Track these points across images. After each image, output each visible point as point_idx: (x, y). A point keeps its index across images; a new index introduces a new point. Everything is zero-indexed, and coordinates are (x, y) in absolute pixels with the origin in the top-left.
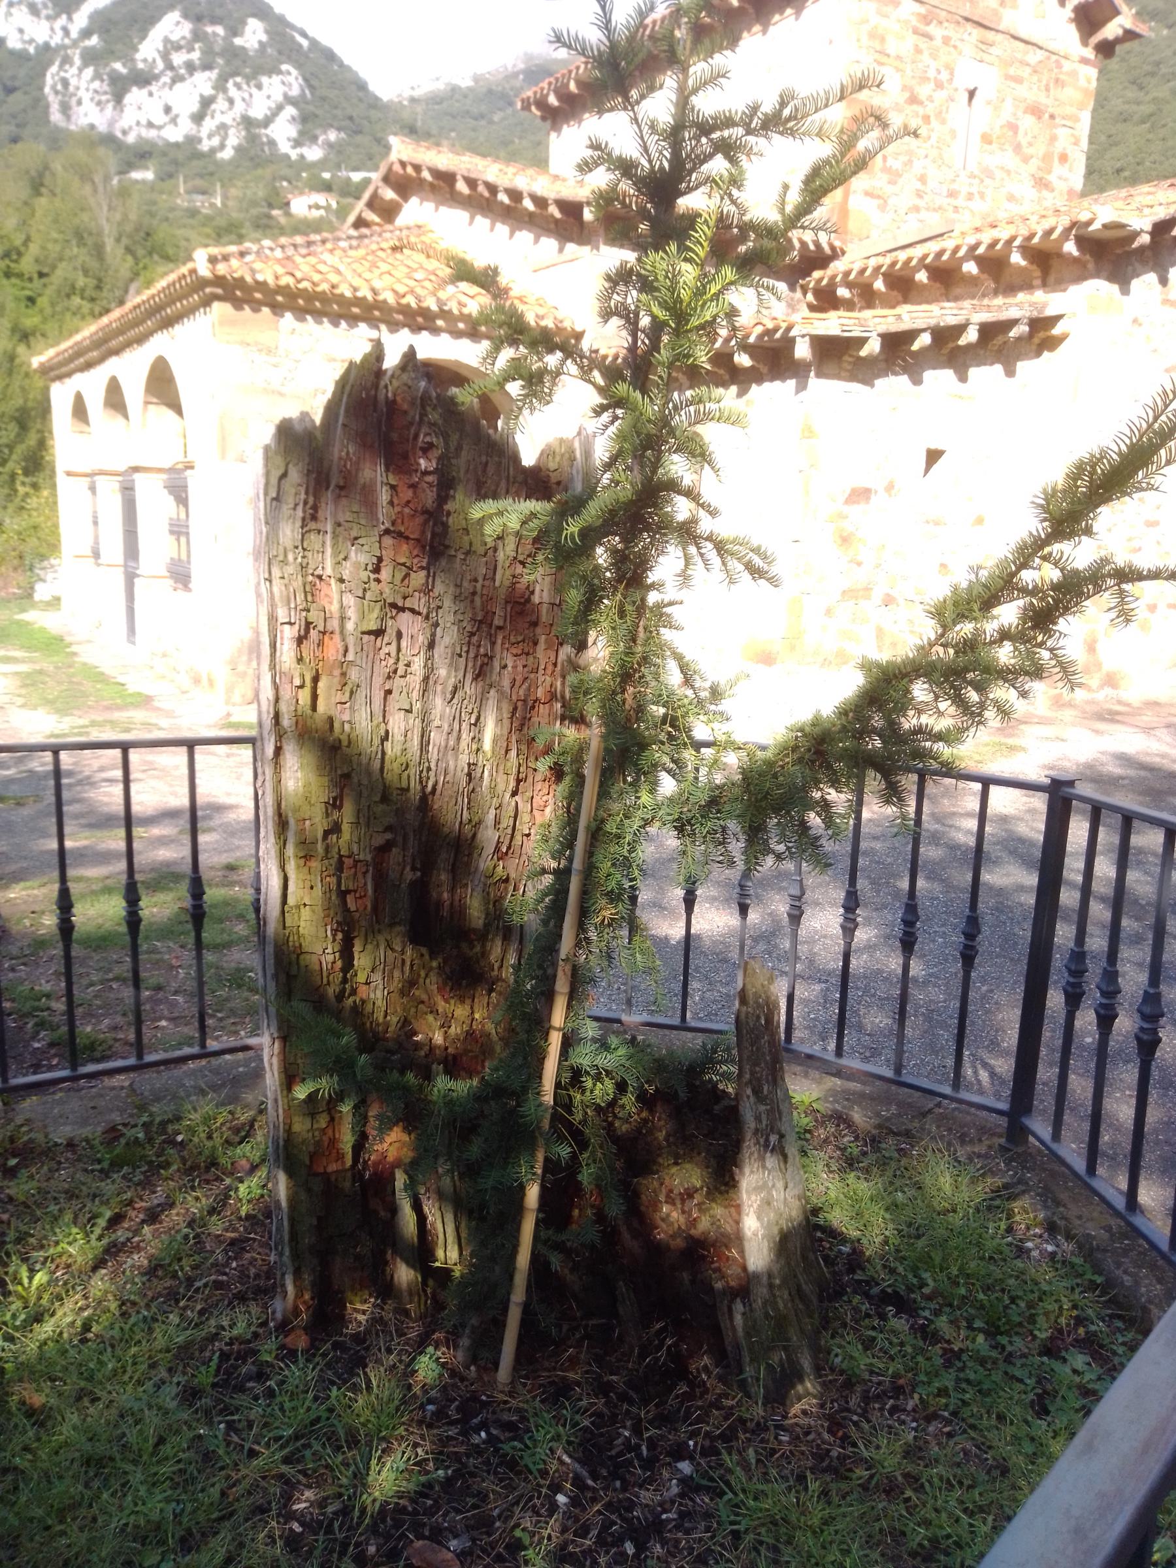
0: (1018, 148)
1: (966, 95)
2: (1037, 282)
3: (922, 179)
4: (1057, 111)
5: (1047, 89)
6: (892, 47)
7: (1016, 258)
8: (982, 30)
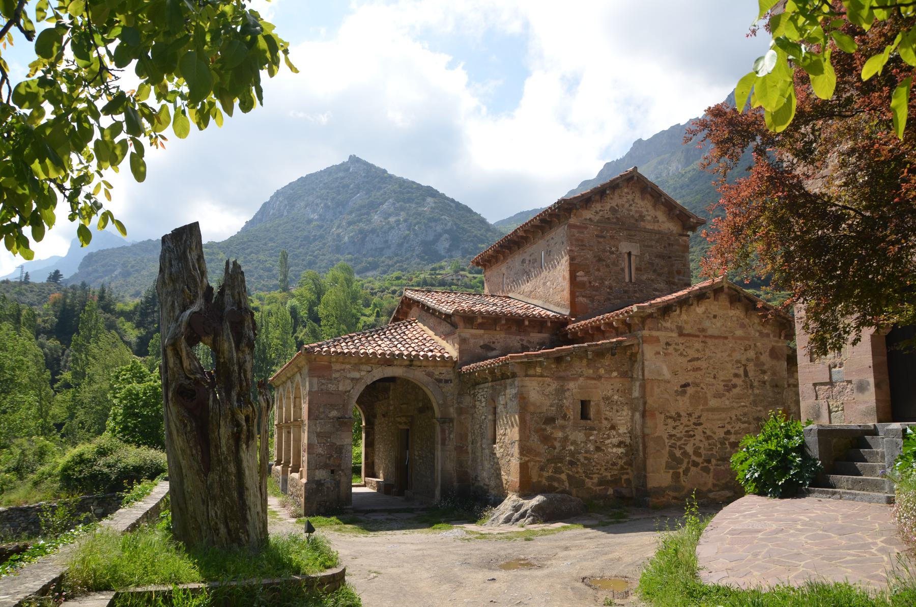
0: (655, 271)
1: (626, 256)
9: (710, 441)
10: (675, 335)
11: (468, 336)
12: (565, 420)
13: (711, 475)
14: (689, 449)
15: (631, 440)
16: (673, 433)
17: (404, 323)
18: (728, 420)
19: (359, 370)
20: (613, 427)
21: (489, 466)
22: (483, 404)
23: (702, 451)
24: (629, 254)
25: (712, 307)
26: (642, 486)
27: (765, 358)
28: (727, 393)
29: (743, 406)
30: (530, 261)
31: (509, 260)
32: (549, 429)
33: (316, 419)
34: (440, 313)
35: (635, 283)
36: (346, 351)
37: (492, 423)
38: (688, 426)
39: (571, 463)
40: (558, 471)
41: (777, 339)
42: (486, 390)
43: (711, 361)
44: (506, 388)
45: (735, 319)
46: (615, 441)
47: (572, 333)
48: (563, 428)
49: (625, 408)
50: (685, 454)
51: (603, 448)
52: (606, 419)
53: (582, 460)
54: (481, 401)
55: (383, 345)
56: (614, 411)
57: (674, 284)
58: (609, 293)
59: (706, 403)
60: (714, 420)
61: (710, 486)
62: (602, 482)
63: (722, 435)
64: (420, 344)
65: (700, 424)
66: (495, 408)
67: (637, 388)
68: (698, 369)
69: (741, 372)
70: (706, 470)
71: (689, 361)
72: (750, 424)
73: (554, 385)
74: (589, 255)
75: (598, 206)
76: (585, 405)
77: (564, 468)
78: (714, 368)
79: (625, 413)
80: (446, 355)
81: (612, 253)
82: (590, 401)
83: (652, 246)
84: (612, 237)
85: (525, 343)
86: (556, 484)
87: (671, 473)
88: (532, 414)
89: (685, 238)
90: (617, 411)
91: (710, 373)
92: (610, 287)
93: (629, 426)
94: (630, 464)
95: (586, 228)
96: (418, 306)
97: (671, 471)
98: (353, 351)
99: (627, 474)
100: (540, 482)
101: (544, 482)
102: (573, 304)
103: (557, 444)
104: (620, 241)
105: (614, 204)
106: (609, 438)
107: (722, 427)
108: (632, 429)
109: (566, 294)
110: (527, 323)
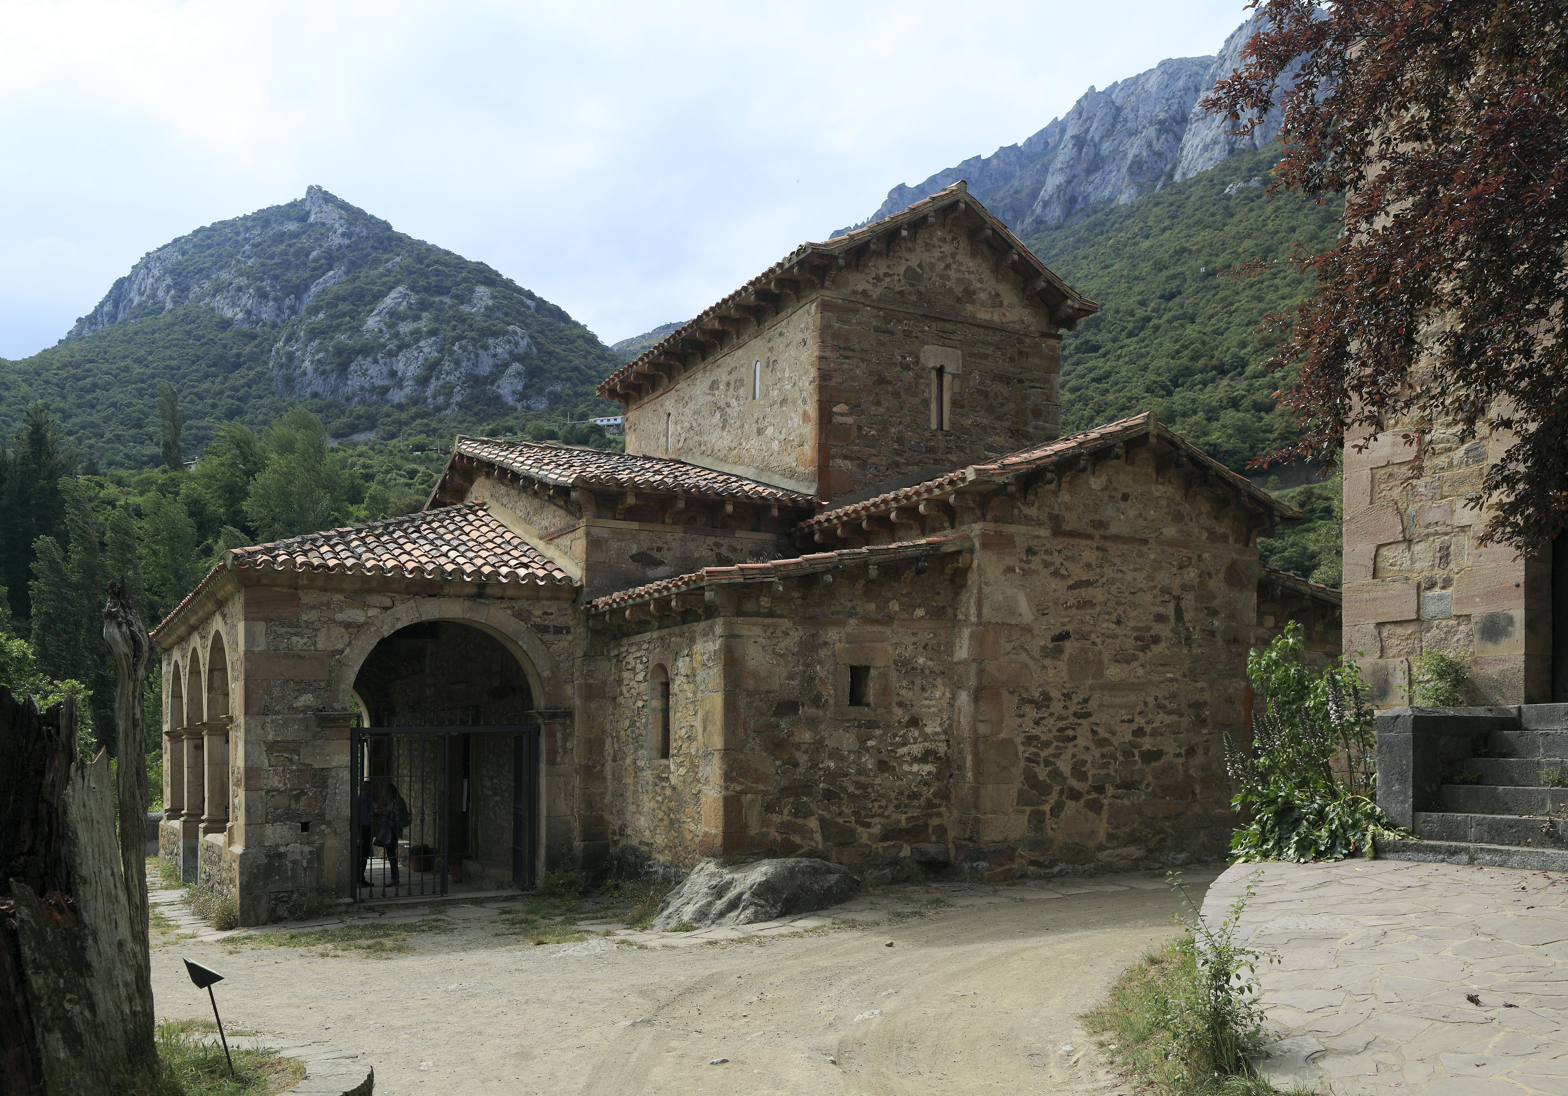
0: (990, 409)
1: (933, 375)
2: (947, 525)
3: (900, 441)
11: (604, 533)
12: (818, 707)
15: (949, 746)
17: (458, 511)
18: (1141, 707)
19: (365, 606)
20: (914, 722)
21: (653, 804)
22: (640, 677)
23: (1091, 771)
26: (970, 839)
29: (1171, 680)
30: (728, 384)
31: (682, 385)
33: (266, 711)
34: (544, 485)
35: (948, 433)
36: (332, 563)
37: (660, 716)
38: (1061, 718)
39: (830, 795)
40: (802, 812)
42: (645, 646)
47: (823, 531)
49: (939, 682)
52: (901, 704)
53: (851, 789)
54: (633, 669)
55: (416, 553)
56: (917, 688)
57: (1026, 436)
58: (897, 453)
60: (1113, 707)
63: (1128, 737)
64: (499, 551)
65: (1088, 715)
66: (666, 685)
67: (966, 643)
72: (1181, 715)
77: (813, 806)
78: (1118, 603)
79: (938, 694)
80: (558, 575)
81: (906, 367)
84: (907, 334)
85: (724, 550)
87: (1028, 813)
88: (750, 694)
90: (923, 689)
91: (1109, 614)
92: (900, 441)
93: (945, 717)
96: (489, 475)
98: (349, 562)
100: (767, 834)
101: (774, 834)
103: (803, 759)
106: (904, 744)
107: (1131, 721)
108: (951, 726)
109: (809, 450)
110: (729, 508)
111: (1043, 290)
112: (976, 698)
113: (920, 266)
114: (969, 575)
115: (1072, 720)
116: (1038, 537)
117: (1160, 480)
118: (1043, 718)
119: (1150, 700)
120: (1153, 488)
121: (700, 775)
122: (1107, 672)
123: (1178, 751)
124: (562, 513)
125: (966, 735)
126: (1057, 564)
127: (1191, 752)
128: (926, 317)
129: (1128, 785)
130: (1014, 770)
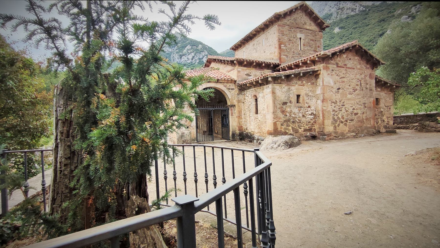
0: (310, 46)
1: (299, 39)
4: (316, 40)
5: (314, 36)
6: (285, 33)
7: (308, 62)
8: (300, 29)
9: (348, 113)
10: (335, 66)
13: (348, 127)
14: (340, 116)
16: (334, 109)
18: (354, 104)
23: (345, 117)
24: (300, 39)
25: (349, 55)
27: (368, 78)
28: (354, 92)
29: (360, 98)
32: (284, 107)
38: (339, 106)
39: (293, 122)
41: (371, 70)
43: (348, 79)
44: (263, 89)
45: (357, 60)
46: (310, 113)
48: (290, 107)
50: (338, 118)
51: (305, 115)
52: (307, 103)
53: (297, 121)
59: (346, 97)
60: (349, 104)
61: (347, 131)
62: (305, 130)
65: (344, 105)
66: (256, 100)
68: (343, 82)
69: (359, 84)
70: (346, 125)
71: (340, 78)
72: (361, 105)
73: (286, 88)
74: (286, 38)
75: (288, 18)
76: (298, 96)
77: (290, 124)
79: (314, 101)
82: (300, 95)
83: (309, 36)
86: (287, 131)
89: (321, 33)
91: (348, 84)
92: (294, 52)
94: (315, 122)
95: (285, 27)
97: (333, 125)
99: (314, 126)
101: (283, 130)
102: (280, 59)
103: (288, 114)
104: (297, 33)
105: (295, 17)
106: (307, 111)
107: (352, 107)
109: (277, 54)
110: (264, 65)
111: (320, 22)
112: (323, 102)
113: (296, 18)
114: (320, 75)
115: (341, 106)
116: (334, 67)
117: (357, 56)
118: (336, 106)
119: (356, 102)
120: (355, 57)
121: (266, 118)
122: (347, 96)
123: (361, 113)
124: (231, 66)
125: (320, 109)
126: (338, 73)
127: (363, 113)
128: (298, 28)
129: (352, 120)
130: (330, 117)
